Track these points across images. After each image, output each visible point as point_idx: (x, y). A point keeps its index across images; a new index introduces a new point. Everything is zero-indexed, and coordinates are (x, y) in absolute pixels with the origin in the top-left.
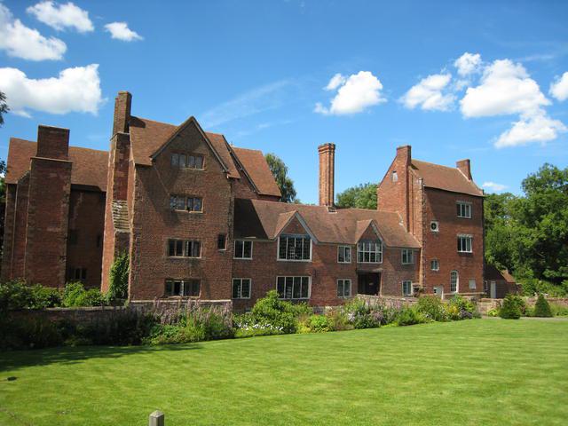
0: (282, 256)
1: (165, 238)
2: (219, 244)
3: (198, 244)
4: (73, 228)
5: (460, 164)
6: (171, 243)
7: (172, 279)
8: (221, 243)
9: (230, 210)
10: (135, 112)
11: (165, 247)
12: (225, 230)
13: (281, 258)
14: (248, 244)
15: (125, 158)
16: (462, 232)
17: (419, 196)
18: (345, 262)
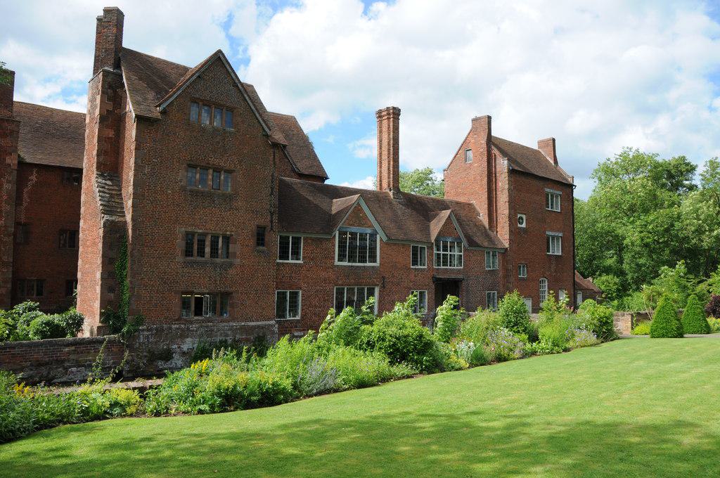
1: (181, 230)
2: (258, 239)
3: (227, 239)
4: (23, 219)
5: (542, 143)
6: (189, 237)
7: (192, 293)
8: (260, 239)
9: (272, 189)
10: (130, 42)
11: (180, 243)
12: (264, 221)
13: (375, 261)
14: (296, 241)
15: (115, 108)
16: (552, 230)
17: (503, 182)
18: (420, 267)
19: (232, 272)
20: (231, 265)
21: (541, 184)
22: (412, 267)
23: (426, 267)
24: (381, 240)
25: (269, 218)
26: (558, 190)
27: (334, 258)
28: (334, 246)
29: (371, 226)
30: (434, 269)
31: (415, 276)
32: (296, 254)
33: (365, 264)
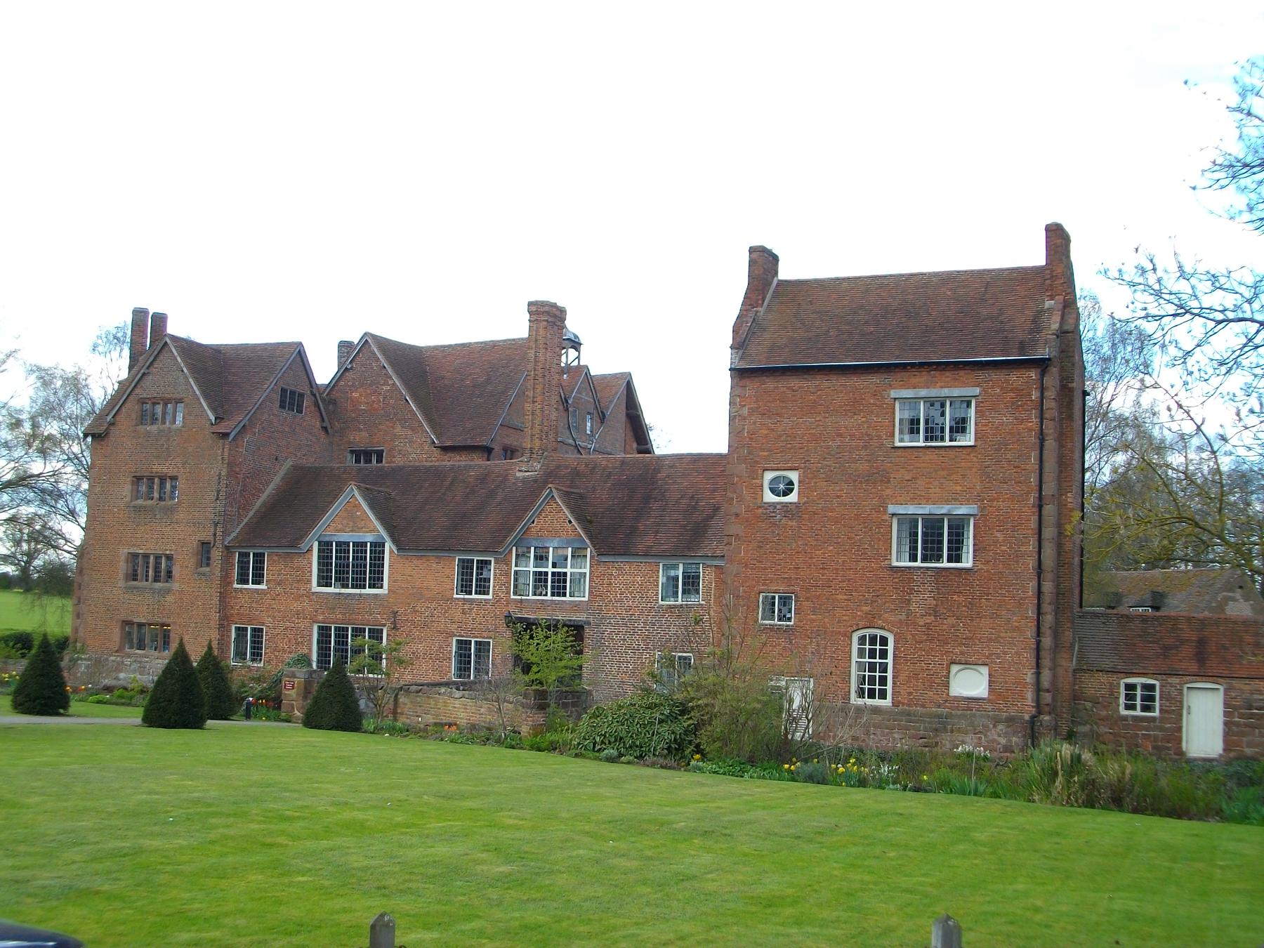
0: (324, 580)
1: (124, 551)
9: (218, 492)
11: (122, 567)
12: (206, 535)
14: (259, 558)
18: (474, 596)
19: (170, 598)
20: (169, 591)
21: (874, 380)
22: (455, 596)
23: (490, 597)
24: (391, 552)
25: (212, 530)
26: (964, 385)
27: (310, 581)
28: (311, 563)
29: (375, 530)
30: (509, 602)
31: (464, 613)
32: (258, 579)
33: (363, 591)
